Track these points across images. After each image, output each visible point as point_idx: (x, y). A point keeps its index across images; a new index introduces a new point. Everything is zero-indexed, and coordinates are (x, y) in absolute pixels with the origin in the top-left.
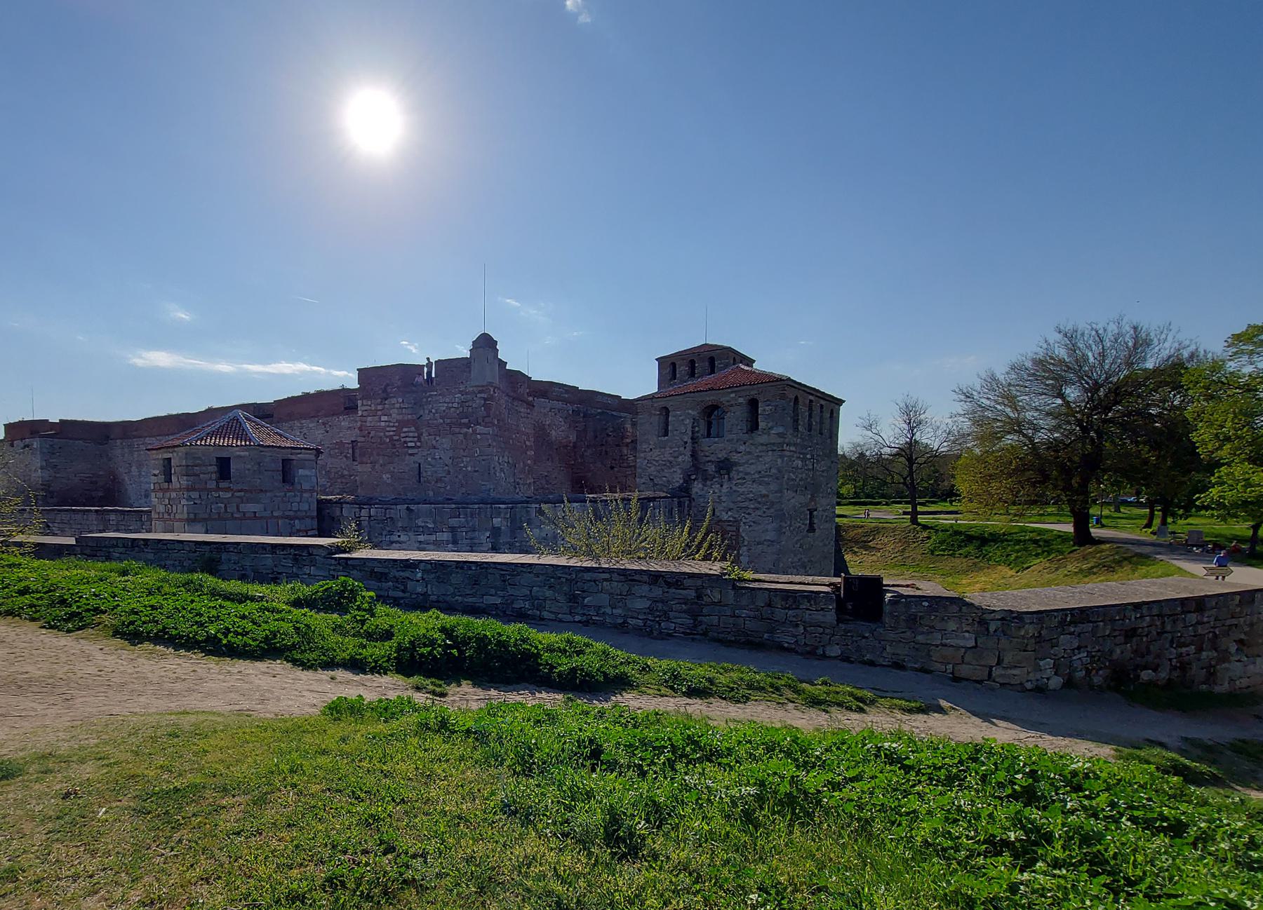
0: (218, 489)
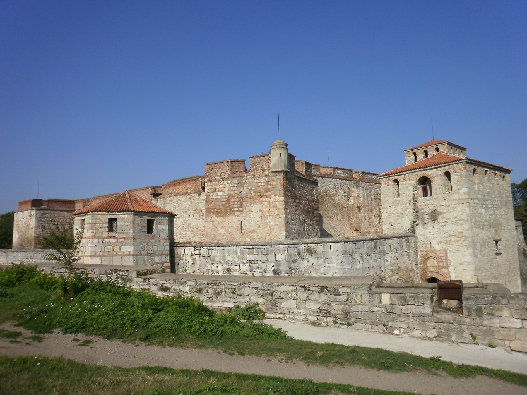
0: (109, 237)
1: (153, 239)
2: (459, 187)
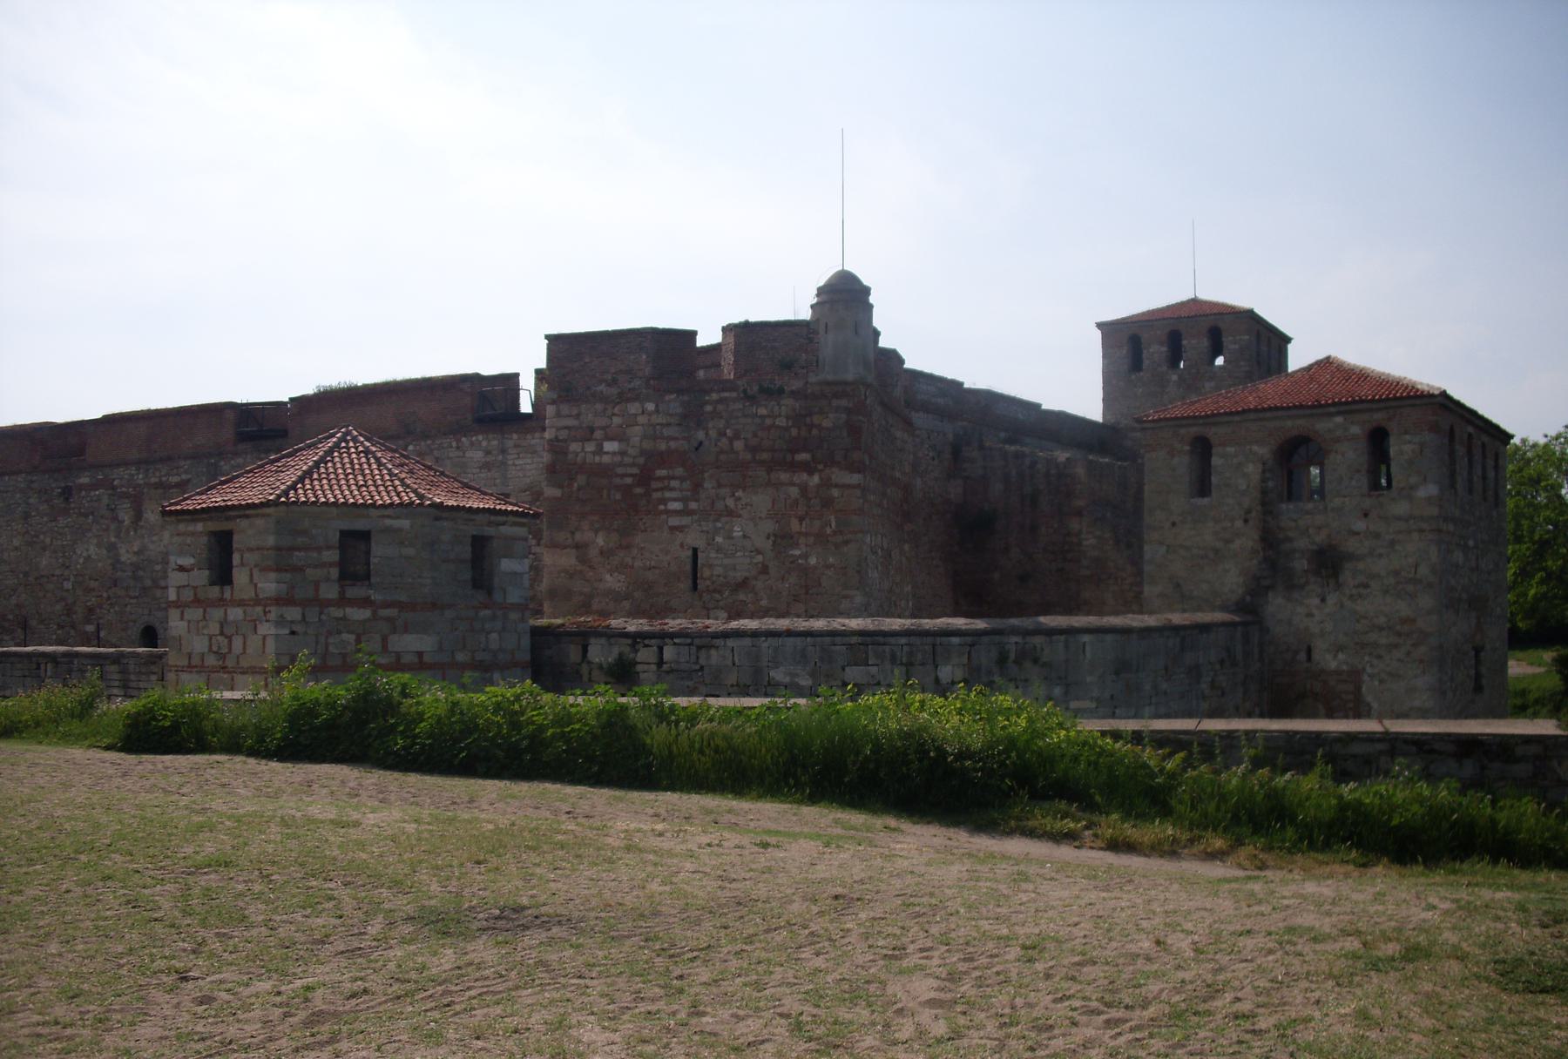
0: (343, 601)
1: (486, 607)
2: (1413, 480)
